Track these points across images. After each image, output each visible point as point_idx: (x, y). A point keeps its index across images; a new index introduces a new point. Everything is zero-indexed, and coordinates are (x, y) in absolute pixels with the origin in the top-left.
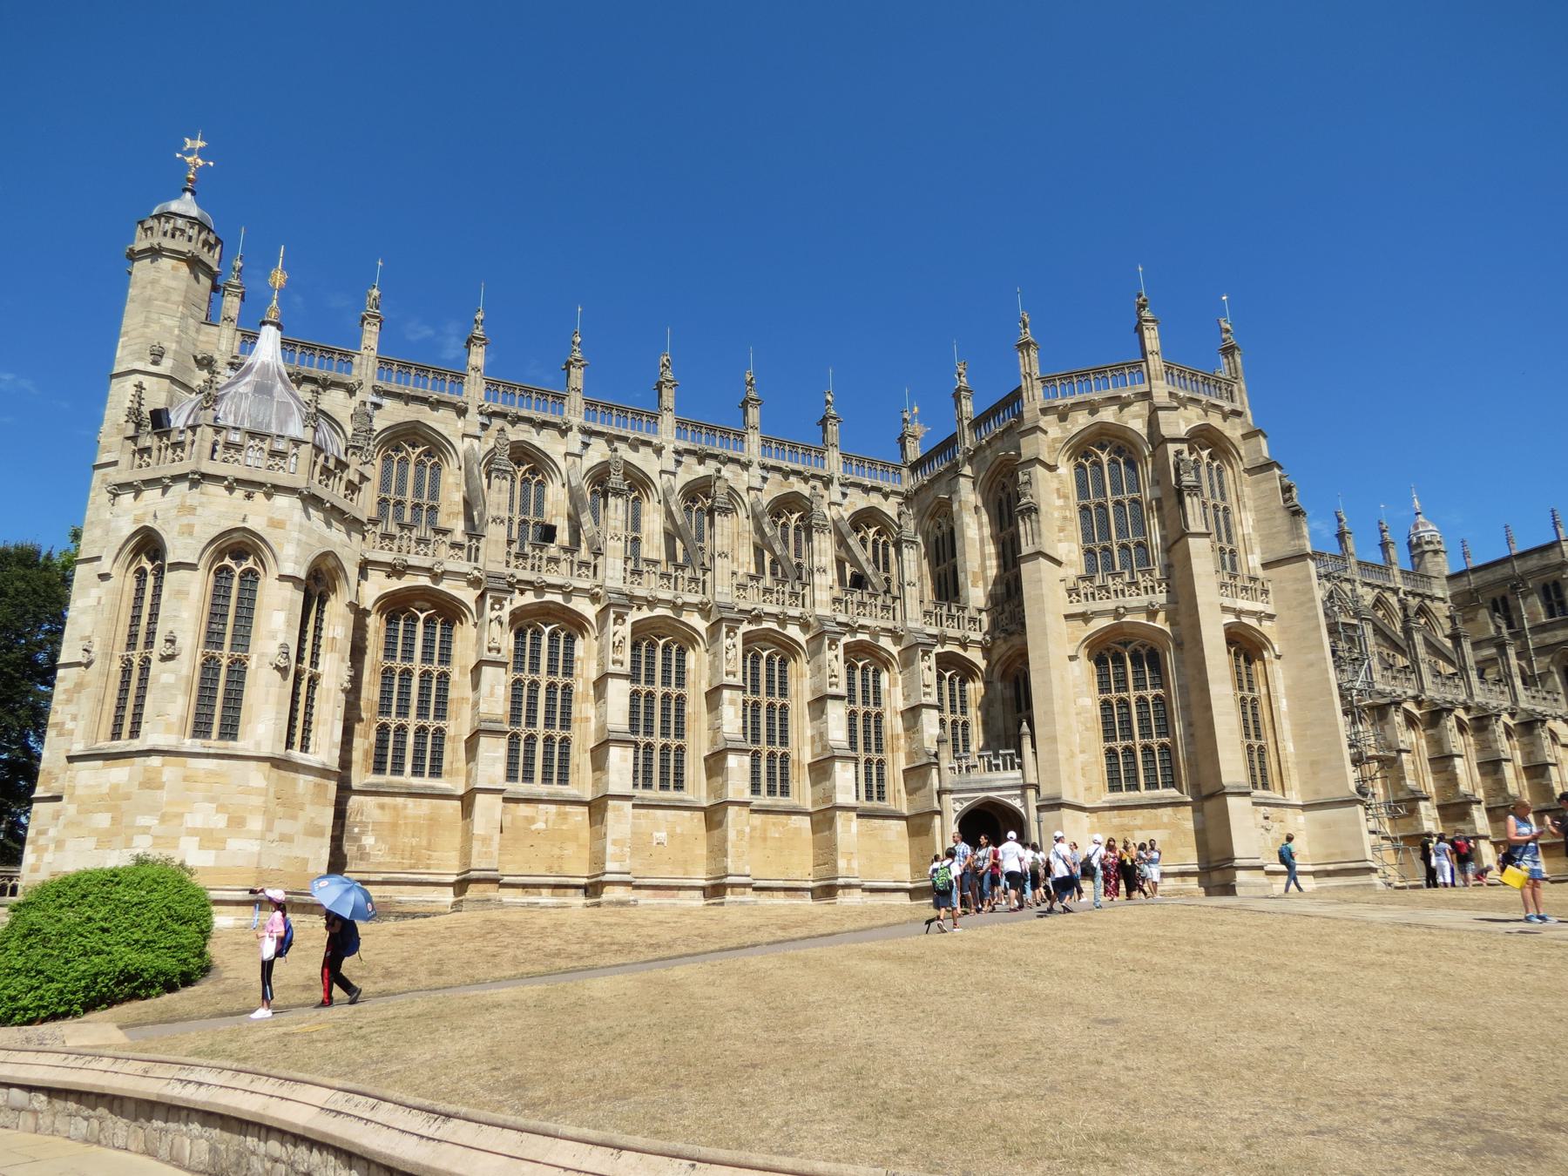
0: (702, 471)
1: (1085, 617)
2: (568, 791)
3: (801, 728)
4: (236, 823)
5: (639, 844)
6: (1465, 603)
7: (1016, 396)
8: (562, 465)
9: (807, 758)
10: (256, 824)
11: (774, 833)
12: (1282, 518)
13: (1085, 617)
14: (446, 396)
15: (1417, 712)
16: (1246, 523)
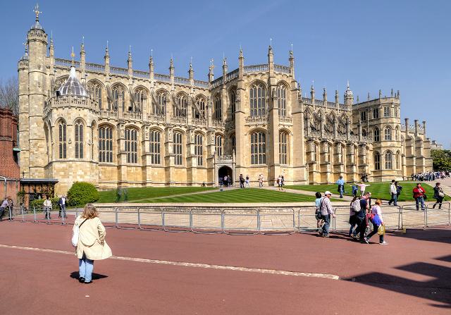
0: (160, 87)
1: (249, 126)
2: (137, 164)
3: (185, 150)
4: (86, 173)
5: (153, 175)
6: (355, 112)
7: (238, 70)
8: (128, 87)
9: (186, 157)
10: (89, 174)
11: (179, 172)
12: (297, 103)
13: (249, 126)
14: (101, 72)
15: (332, 143)
16: (289, 104)
